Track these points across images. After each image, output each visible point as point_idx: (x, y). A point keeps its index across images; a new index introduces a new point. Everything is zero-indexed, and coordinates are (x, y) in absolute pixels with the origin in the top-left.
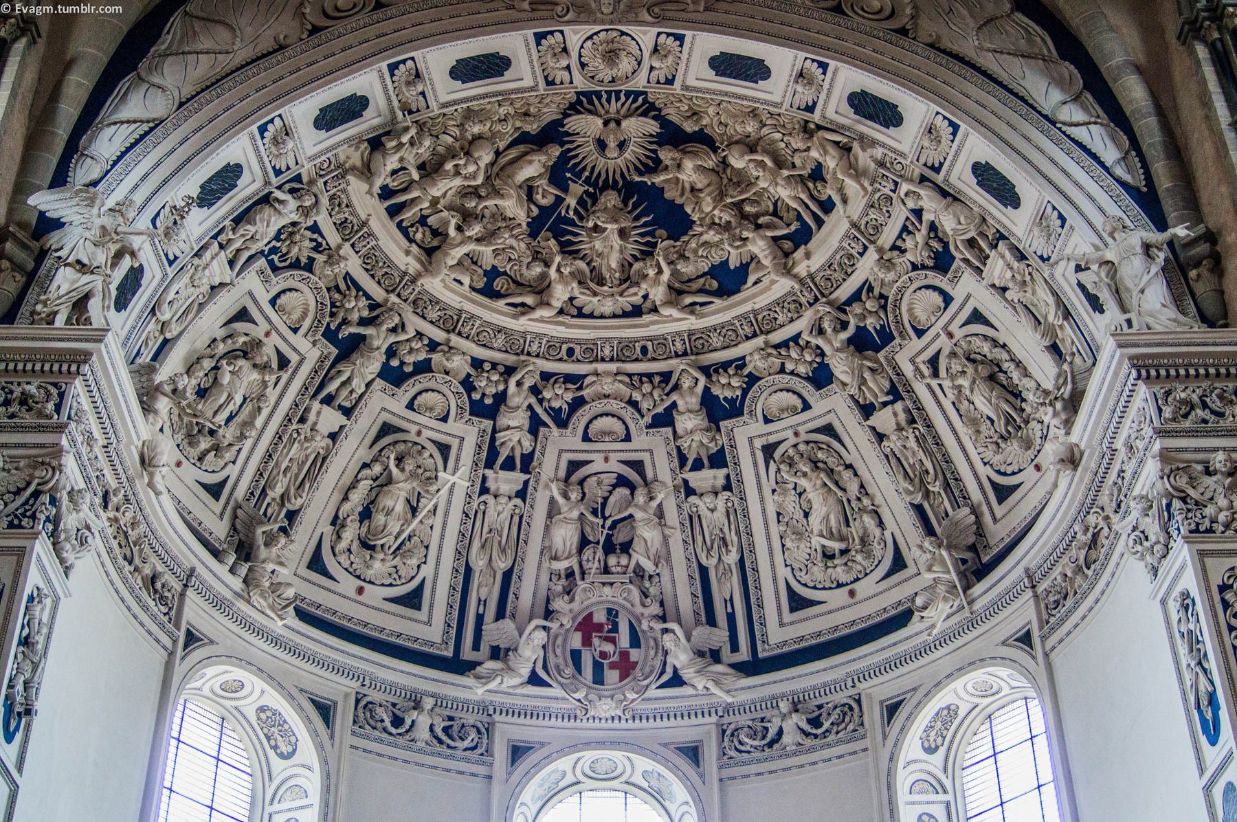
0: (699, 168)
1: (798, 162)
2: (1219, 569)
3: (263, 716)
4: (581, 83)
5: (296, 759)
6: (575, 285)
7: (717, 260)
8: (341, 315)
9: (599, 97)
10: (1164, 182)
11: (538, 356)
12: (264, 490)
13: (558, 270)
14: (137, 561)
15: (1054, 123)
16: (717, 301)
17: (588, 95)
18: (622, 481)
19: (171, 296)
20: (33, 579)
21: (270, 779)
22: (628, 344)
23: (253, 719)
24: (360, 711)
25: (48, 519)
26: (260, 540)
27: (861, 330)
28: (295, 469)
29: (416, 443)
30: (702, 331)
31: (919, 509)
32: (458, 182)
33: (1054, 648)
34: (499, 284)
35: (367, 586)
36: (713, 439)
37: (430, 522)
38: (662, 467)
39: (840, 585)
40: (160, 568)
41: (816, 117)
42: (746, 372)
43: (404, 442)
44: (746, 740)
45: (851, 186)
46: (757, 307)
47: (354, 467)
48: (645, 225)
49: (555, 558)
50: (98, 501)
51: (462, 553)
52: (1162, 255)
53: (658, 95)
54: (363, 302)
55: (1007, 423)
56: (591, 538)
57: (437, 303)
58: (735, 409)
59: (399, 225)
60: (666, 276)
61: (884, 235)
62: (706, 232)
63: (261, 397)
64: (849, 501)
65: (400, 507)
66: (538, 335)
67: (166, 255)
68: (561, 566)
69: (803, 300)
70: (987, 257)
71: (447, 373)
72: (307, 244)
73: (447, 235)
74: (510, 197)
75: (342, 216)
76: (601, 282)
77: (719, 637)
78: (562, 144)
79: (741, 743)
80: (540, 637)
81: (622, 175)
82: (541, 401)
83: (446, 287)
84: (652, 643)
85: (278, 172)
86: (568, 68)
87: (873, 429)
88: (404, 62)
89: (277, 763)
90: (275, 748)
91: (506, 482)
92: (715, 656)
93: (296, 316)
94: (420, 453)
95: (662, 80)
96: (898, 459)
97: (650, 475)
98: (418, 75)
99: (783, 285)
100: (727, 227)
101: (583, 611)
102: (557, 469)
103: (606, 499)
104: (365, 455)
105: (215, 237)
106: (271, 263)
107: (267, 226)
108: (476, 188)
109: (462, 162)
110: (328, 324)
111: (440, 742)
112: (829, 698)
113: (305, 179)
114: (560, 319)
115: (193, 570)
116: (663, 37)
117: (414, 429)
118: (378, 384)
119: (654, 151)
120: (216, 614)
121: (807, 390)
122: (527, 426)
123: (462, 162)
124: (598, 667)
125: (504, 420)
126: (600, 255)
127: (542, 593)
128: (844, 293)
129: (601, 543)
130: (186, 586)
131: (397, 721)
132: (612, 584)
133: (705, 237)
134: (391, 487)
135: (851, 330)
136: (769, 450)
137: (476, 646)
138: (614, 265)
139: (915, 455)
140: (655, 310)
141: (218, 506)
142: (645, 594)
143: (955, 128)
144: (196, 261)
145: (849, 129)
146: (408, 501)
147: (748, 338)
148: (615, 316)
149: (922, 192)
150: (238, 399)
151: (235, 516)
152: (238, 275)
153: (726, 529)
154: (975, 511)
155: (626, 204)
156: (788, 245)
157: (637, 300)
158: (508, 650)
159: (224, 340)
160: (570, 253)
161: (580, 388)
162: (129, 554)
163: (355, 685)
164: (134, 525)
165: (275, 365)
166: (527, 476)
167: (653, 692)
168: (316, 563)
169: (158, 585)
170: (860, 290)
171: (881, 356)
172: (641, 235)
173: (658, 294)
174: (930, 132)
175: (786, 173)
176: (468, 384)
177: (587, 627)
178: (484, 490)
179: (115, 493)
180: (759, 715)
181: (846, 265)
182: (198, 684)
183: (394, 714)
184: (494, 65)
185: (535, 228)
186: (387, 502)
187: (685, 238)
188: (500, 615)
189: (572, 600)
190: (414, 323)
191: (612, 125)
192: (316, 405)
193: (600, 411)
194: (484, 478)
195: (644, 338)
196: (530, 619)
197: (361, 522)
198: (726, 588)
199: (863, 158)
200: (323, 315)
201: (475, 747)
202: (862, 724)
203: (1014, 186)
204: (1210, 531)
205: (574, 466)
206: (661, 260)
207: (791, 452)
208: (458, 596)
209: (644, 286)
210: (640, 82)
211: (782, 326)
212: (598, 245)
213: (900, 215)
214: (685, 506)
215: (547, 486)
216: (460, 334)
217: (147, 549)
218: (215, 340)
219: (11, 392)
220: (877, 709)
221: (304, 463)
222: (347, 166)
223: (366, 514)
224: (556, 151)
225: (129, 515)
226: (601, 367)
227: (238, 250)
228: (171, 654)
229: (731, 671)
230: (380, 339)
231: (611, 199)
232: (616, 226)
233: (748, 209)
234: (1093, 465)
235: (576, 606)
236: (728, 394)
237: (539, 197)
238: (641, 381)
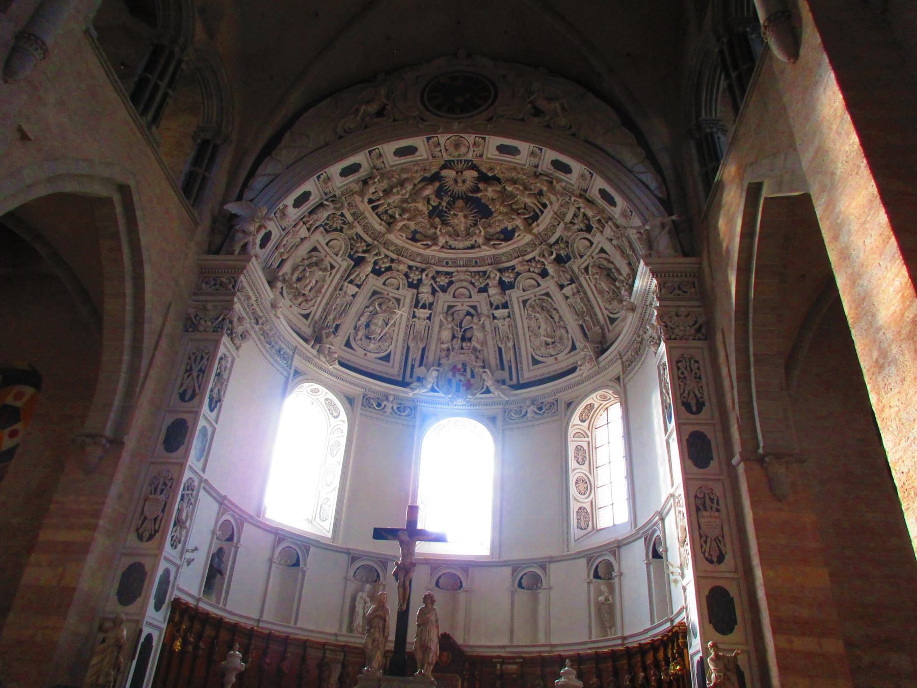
0: (494, 191)
1: (533, 188)
3: (327, 402)
4: (446, 157)
5: (339, 419)
6: (447, 237)
7: (503, 227)
8: (355, 249)
9: (454, 163)
11: (434, 264)
12: (326, 316)
13: (440, 231)
14: (273, 343)
16: (503, 243)
17: (449, 161)
18: (468, 314)
19: (284, 243)
20: (222, 350)
21: (330, 426)
22: (470, 260)
23: (324, 403)
24: (365, 400)
25: (228, 329)
26: (324, 336)
27: (558, 256)
28: (339, 308)
29: (387, 299)
30: (498, 255)
31: (581, 327)
32: (399, 197)
33: (627, 383)
34: (418, 236)
35: (369, 354)
36: (503, 297)
37: (393, 329)
38: (484, 309)
39: (552, 356)
40: (283, 346)
41: (539, 169)
42: (515, 271)
43: (382, 298)
44: (513, 415)
45: (553, 198)
46: (519, 245)
47: (363, 307)
48: (475, 213)
49: (443, 343)
50: (253, 321)
51: (406, 339)
52: (668, 228)
53: (476, 161)
54: (364, 244)
55: (613, 293)
56: (456, 335)
57: (394, 243)
58: (511, 286)
59: (377, 214)
60: (483, 233)
61: (567, 216)
62: (498, 216)
63: (324, 280)
64: (555, 322)
65: (380, 322)
66: (433, 257)
67: (281, 227)
68: (445, 346)
69: (537, 243)
70: (605, 227)
71: (398, 271)
72: (340, 222)
73: (396, 218)
74: (420, 202)
75: (353, 211)
76: (458, 236)
77: (505, 375)
78: (440, 182)
79: (512, 416)
80: (435, 374)
81: (465, 193)
82: (436, 282)
83: (397, 238)
84: (479, 377)
85: (326, 194)
86: (440, 151)
87: (564, 294)
88: (374, 150)
90: (332, 414)
91: (423, 313)
92: (504, 382)
93: (336, 250)
94: (389, 302)
95: (478, 155)
96: (574, 307)
97: (479, 311)
98: (380, 155)
99: (528, 238)
100: (506, 214)
101: (453, 363)
102: (443, 309)
103: (462, 320)
104: (366, 303)
105: (301, 219)
106: (326, 230)
107: (323, 215)
108: (407, 199)
109: (399, 189)
110: (350, 253)
111: (396, 413)
112: (546, 400)
113: (337, 196)
114: (442, 250)
115: (296, 347)
116: (477, 139)
117: (386, 293)
118: (372, 275)
119: (477, 184)
120: (307, 364)
121: (539, 279)
122: (430, 291)
123: (399, 189)
125: (422, 289)
126: (457, 225)
127: (437, 357)
128: (553, 240)
129: (460, 337)
130: (294, 353)
131: (379, 405)
132: (464, 354)
133: (498, 218)
134: (377, 316)
135: (554, 256)
136: (525, 302)
137: (411, 377)
138: (462, 229)
139: (580, 306)
140: (479, 247)
141: (308, 323)
142: (477, 358)
143: (592, 175)
144: (294, 229)
145: (552, 174)
146: (384, 321)
147: (516, 258)
148: (464, 249)
149: (580, 200)
150: (314, 282)
151: (314, 327)
152: (312, 234)
153: (508, 333)
154: (602, 328)
155: (466, 205)
156: (530, 221)
157: (473, 242)
158: (423, 378)
159: (307, 259)
160: (445, 224)
161: (451, 277)
162: (269, 341)
163: (363, 390)
164: (271, 330)
165: (329, 268)
166: (431, 312)
167: (478, 395)
168: (348, 344)
169: (282, 352)
170: (558, 240)
171: (567, 265)
172: (474, 217)
173: (480, 241)
174: (582, 176)
175: (527, 193)
178: (414, 317)
179: (261, 318)
180: (519, 405)
181: (553, 228)
182: (301, 390)
183: (379, 403)
184: (411, 150)
185: (431, 214)
186: (375, 321)
187: (491, 218)
188: (421, 365)
189: (449, 360)
190: (384, 251)
191: (459, 173)
192: (346, 284)
193: (459, 286)
194: (414, 312)
195: (476, 258)
196: (433, 366)
197: (366, 328)
198: (508, 356)
199: (558, 187)
200: (348, 249)
201: (409, 416)
202: (557, 410)
203: (614, 198)
204: (675, 339)
205: (450, 307)
206: (480, 227)
207: (533, 303)
208: (404, 357)
209: (475, 237)
210: (470, 156)
211: (529, 253)
212: (456, 221)
213: (572, 210)
214: (493, 323)
215: (439, 316)
216: (403, 256)
217: (277, 339)
218: (304, 259)
219: (217, 280)
220: (563, 404)
221: (342, 306)
222: (354, 191)
223: (367, 326)
224: (437, 185)
225: (268, 327)
226: (459, 269)
227: (311, 225)
228: (287, 379)
229: (509, 388)
230: (370, 258)
231: (460, 203)
232: (462, 214)
233: (514, 206)
234: (640, 312)
235: (450, 362)
236: (509, 280)
237: (432, 202)
238: (475, 275)
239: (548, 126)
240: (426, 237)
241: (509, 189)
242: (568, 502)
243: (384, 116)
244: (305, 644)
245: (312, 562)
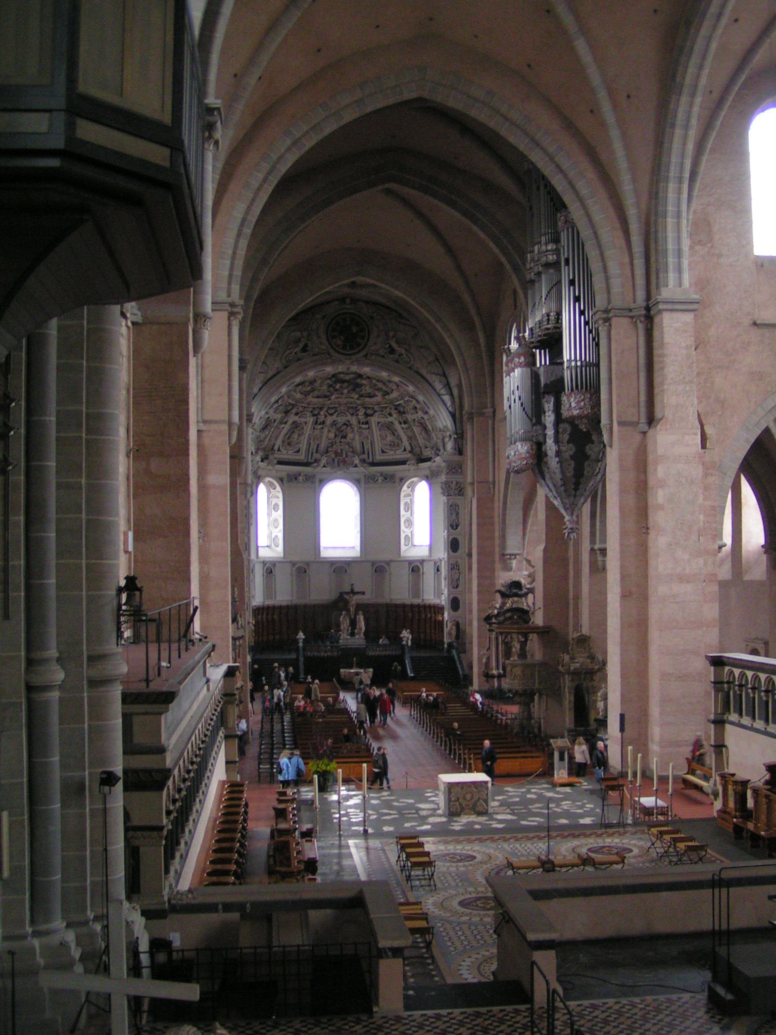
2: (450, 503)
10: (457, 415)
15: (439, 395)
18: (345, 424)
51: (309, 439)
58: (372, 415)
89: (272, 490)
91: (320, 427)
124: (338, 462)
136: (378, 423)
167: (351, 468)
168: (279, 450)
176: (312, 412)
177: (336, 454)
178: (314, 428)
198: (367, 446)
224: (334, 379)
230: (294, 411)
239: (397, 361)
240: (326, 397)
241: (374, 381)
242: (400, 534)
243: (307, 351)
244: (281, 607)
245: (277, 571)
